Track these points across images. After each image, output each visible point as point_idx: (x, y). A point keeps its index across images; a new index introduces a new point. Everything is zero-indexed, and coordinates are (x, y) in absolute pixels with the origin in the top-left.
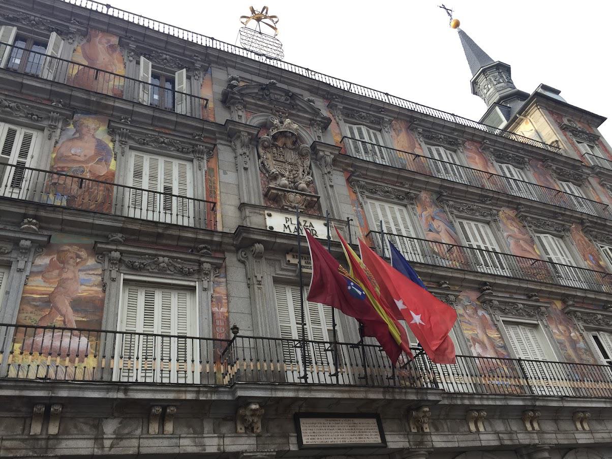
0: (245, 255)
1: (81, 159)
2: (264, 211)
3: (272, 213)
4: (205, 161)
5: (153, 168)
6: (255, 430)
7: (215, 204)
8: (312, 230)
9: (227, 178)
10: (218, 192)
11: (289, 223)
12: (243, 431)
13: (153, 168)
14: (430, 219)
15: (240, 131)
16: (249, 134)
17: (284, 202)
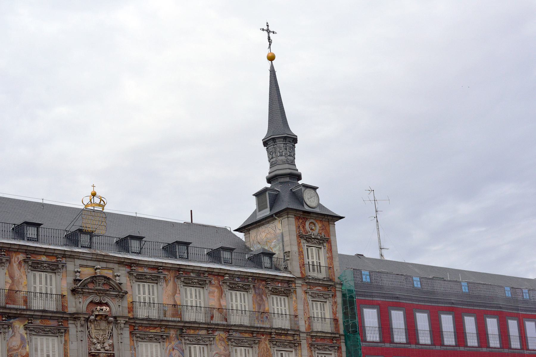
1: (16, 348)
5: (42, 344)
9: (73, 346)
13: (42, 344)
14: (172, 349)
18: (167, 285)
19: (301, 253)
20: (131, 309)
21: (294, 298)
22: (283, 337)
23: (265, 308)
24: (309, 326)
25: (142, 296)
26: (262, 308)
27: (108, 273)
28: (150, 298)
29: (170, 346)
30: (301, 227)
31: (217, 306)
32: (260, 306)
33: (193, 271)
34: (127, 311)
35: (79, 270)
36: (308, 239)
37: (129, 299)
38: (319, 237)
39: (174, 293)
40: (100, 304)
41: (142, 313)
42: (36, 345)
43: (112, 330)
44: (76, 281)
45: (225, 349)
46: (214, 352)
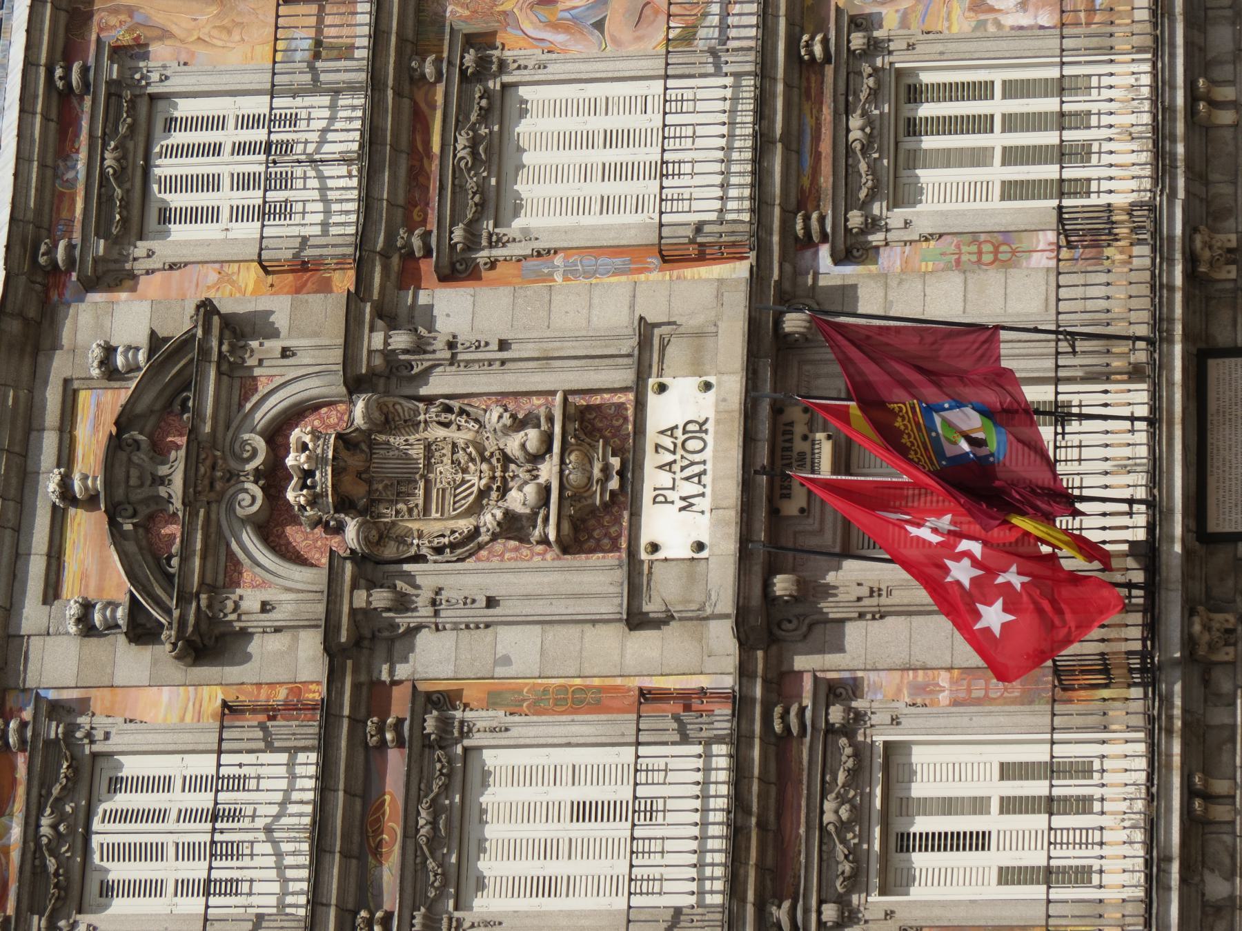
0: (790, 622)
2: (643, 562)
3: (645, 539)
4: (469, 715)
5: (514, 850)
6: (1230, 626)
7: (641, 690)
8: (685, 432)
9: (521, 652)
10: (578, 681)
11: (671, 495)
12: (1231, 649)
13: (514, 850)
15: (353, 612)
16: (354, 586)
17: (590, 501)
18: (165, 35)
20: (303, 269)
25: (226, 198)
27: (98, 413)
28: (241, 148)
34: (316, 301)
35: (73, 610)
37: (243, 293)
40: (273, 477)
41: (326, 206)
42: (517, 886)
43: (429, 400)
44: (141, 631)
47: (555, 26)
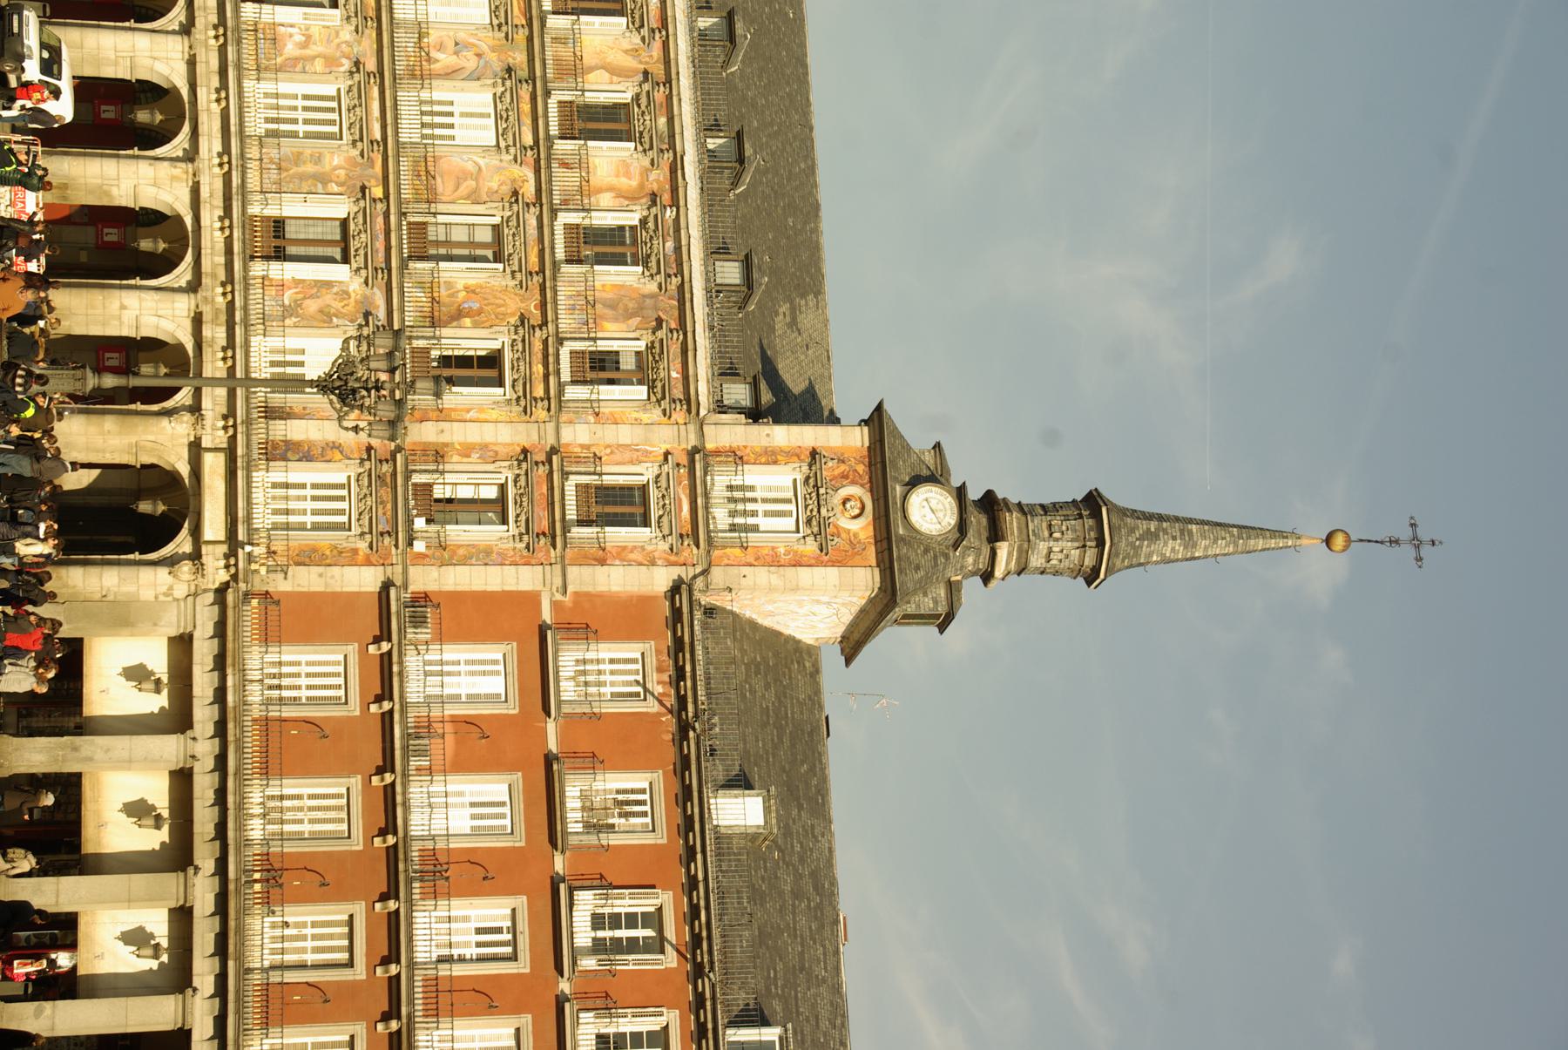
18: (626, 52)
19: (771, 457)
21: (646, 417)
22: (539, 369)
23: (606, 320)
24: (578, 460)
26: (609, 312)
29: (485, 48)
30: (843, 467)
31: (595, 181)
32: (612, 305)
33: (671, 120)
36: (814, 483)
38: (824, 511)
39: (615, 71)
45: (491, 193)
46: (482, 162)
47: (474, 45)
